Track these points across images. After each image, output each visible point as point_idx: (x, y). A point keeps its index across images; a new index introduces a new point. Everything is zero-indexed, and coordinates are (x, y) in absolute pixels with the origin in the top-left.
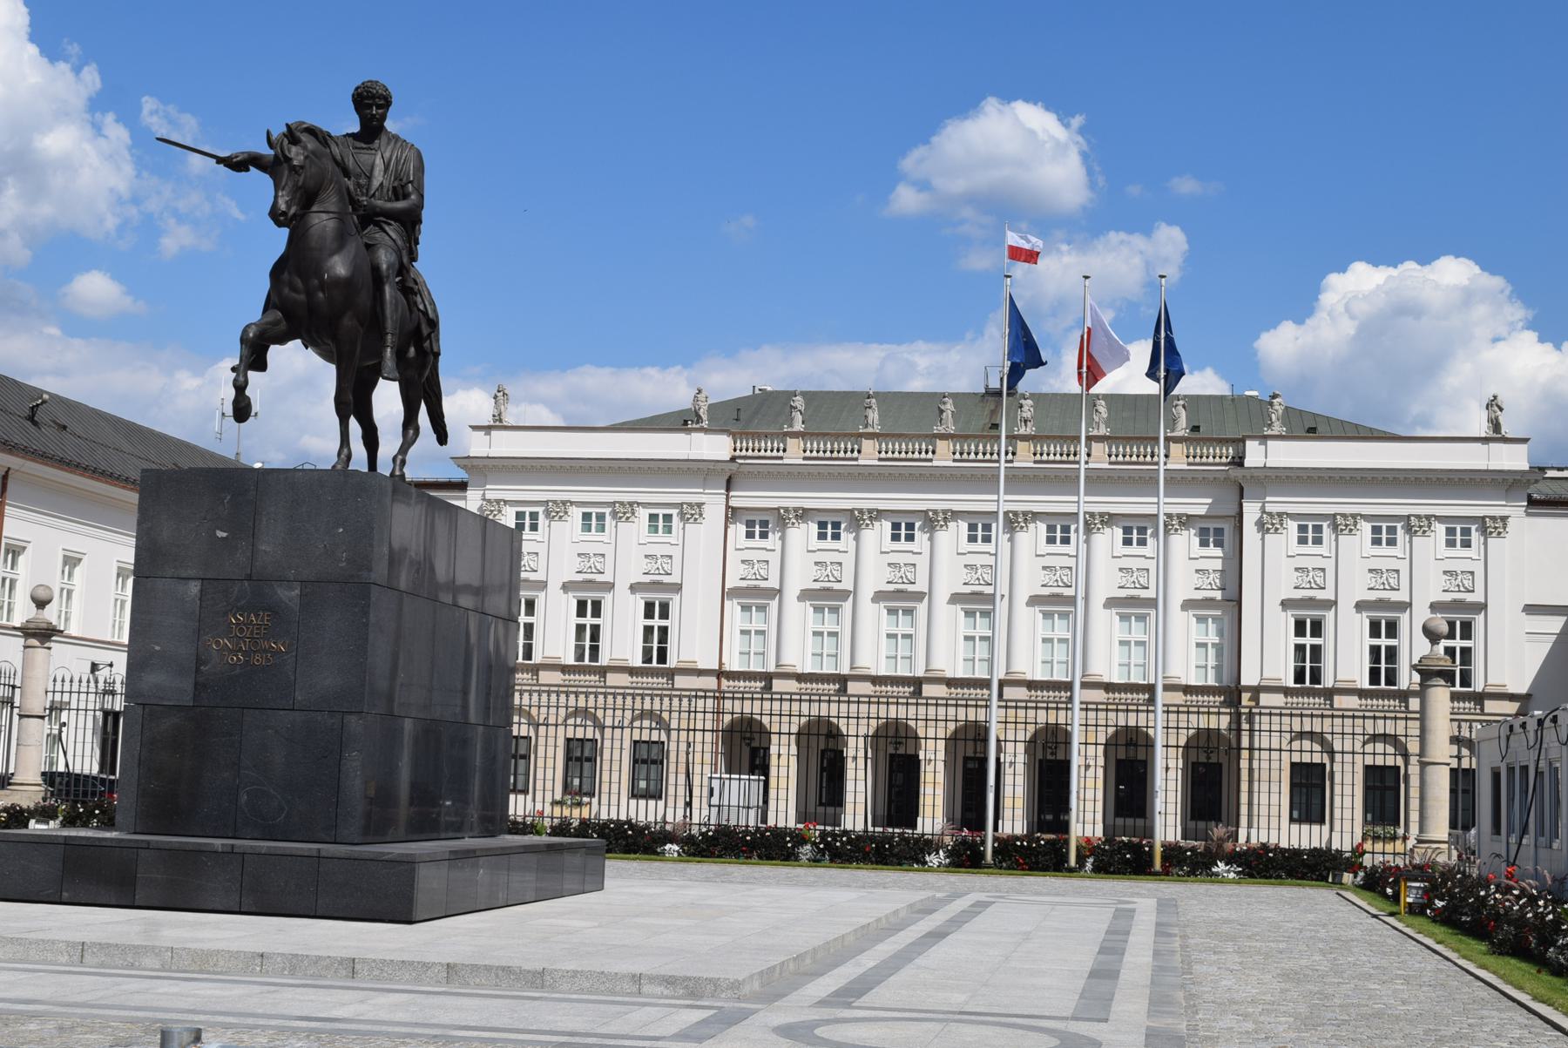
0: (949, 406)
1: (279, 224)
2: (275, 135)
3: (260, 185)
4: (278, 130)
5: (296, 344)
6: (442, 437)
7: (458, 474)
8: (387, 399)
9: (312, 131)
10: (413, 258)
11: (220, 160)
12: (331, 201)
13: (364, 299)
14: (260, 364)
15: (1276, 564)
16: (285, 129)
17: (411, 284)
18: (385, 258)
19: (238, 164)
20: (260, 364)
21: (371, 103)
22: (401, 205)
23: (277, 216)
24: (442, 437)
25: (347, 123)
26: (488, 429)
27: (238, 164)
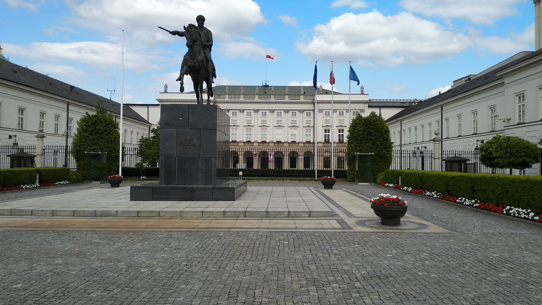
7: (158, 103)
11: (170, 32)
12: (198, 43)
13: (205, 65)
15: (321, 119)
27: (174, 33)
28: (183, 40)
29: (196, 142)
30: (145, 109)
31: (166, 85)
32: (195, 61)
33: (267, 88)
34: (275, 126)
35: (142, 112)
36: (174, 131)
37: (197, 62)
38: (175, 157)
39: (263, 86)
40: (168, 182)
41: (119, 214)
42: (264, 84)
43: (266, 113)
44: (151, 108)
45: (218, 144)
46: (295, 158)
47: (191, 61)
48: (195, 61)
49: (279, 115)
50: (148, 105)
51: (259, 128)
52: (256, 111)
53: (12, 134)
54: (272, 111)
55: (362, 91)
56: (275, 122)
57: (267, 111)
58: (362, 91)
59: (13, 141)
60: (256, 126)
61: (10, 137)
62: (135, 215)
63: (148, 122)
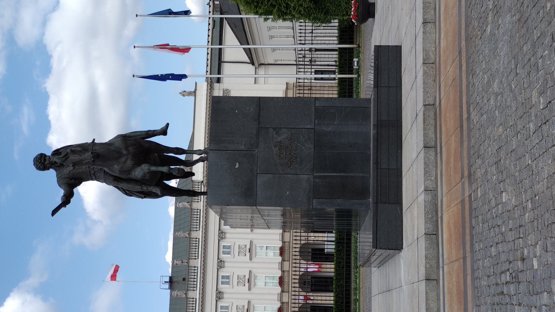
0: (175, 293)
29: (284, 136)
32: (124, 152)
33: (174, 280)
34: (251, 259)
36: (261, 180)
37: (126, 148)
38: (315, 177)
39: (171, 288)
40: (363, 193)
41: (431, 186)
42: (167, 286)
43: (223, 277)
45: (290, 95)
46: (313, 250)
47: (123, 159)
48: (124, 152)
49: (228, 250)
51: (253, 290)
52: (219, 295)
54: (221, 264)
55: (190, 94)
56: (242, 258)
57: (221, 274)
58: (190, 94)
60: (249, 297)
62: (432, 152)
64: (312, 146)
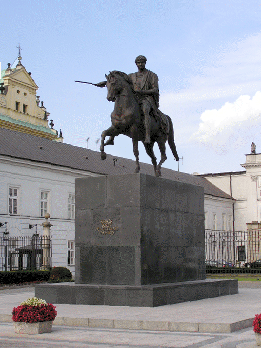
1: (109, 101)
2: (107, 75)
3: (105, 91)
4: (108, 73)
5: (121, 136)
6: (177, 159)
7: (244, 170)
8: (156, 147)
9: (118, 73)
10: (158, 106)
11: (96, 85)
13: (138, 120)
14: (111, 142)
16: (109, 73)
17: (157, 114)
18: (146, 107)
19: (101, 85)
20: (111, 142)
21: (141, 61)
22: (151, 91)
23: (110, 99)
24: (177, 159)
25: (131, 69)
26: (251, 154)
27: (101, 85)
28: (105, 91)
30: (227, 178)
31: (253, 143)
35: (221, 184)
37: (125, 118)
44: (234, 178)
47: (118, 117)
48: (122, 117)
50: (231, 174)
53: (33, 223)
59: (33, 231)
61: (31, 227)
63: (231, 199)
64: (110, 245)
